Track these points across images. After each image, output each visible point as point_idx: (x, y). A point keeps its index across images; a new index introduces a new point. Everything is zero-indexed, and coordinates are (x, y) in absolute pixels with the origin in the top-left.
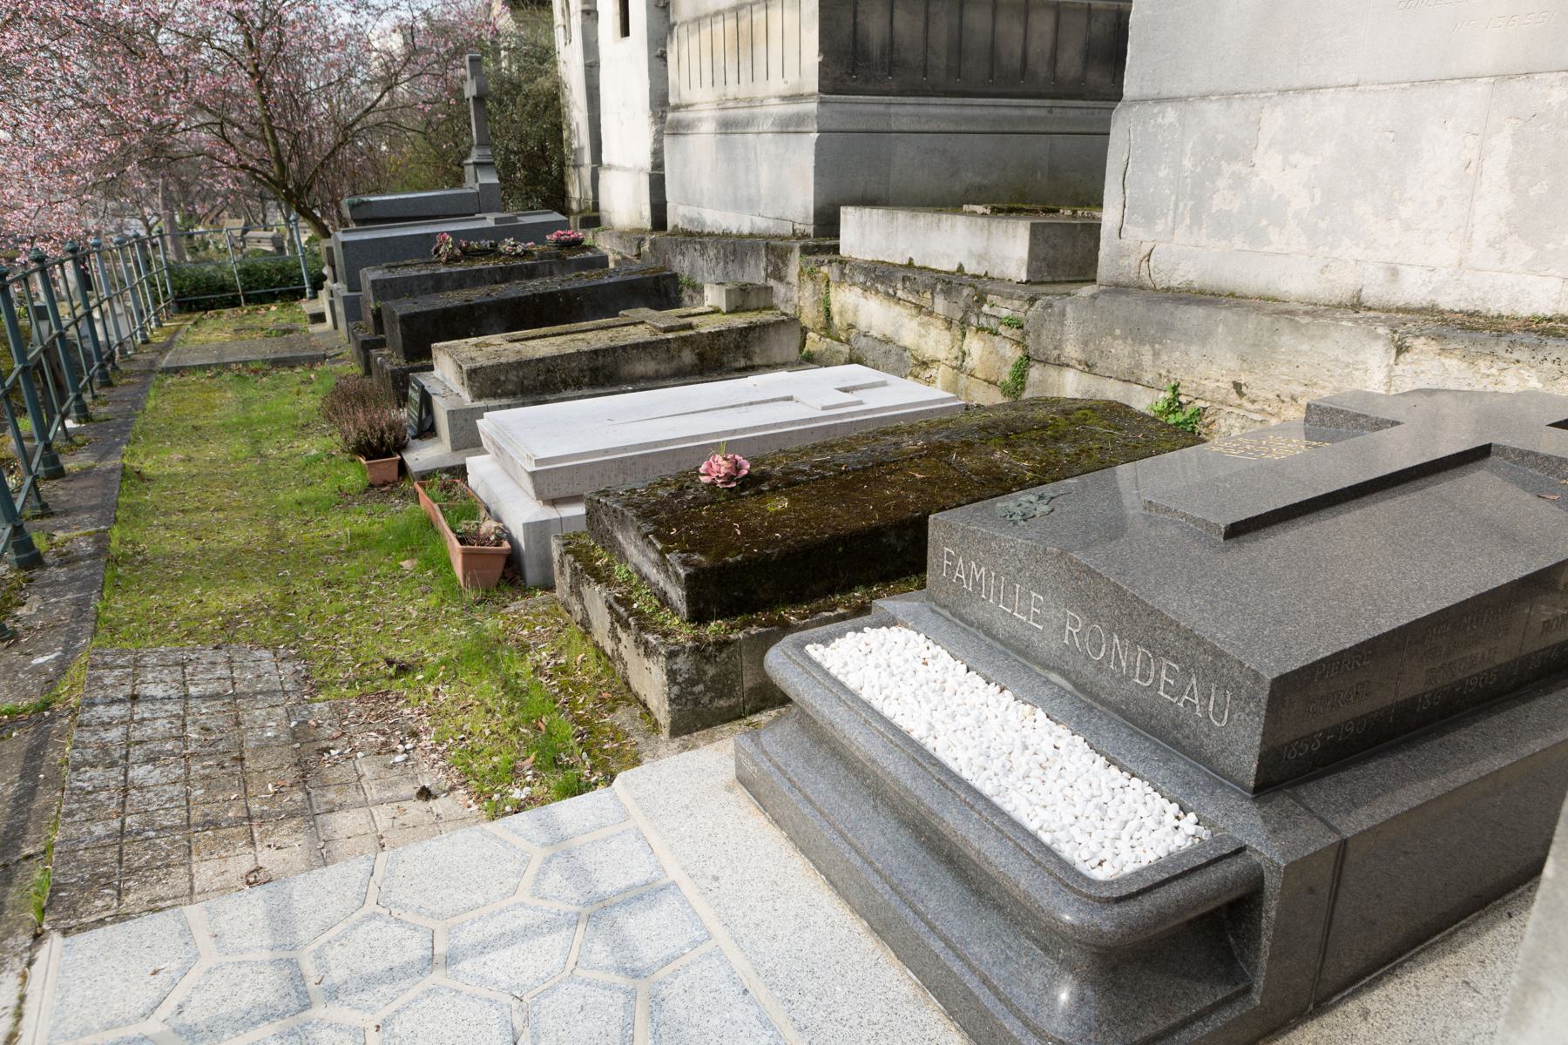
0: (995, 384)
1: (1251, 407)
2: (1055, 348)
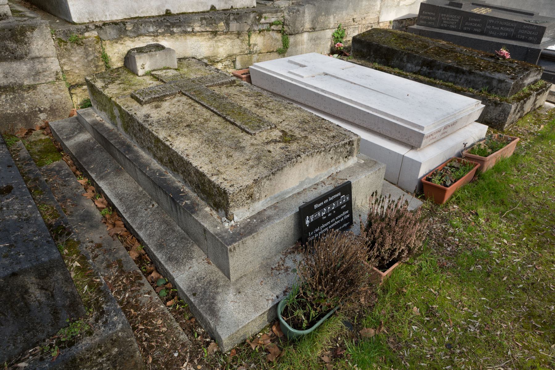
0: (273, 51)
1: (356, 24)
2: (302, 27)
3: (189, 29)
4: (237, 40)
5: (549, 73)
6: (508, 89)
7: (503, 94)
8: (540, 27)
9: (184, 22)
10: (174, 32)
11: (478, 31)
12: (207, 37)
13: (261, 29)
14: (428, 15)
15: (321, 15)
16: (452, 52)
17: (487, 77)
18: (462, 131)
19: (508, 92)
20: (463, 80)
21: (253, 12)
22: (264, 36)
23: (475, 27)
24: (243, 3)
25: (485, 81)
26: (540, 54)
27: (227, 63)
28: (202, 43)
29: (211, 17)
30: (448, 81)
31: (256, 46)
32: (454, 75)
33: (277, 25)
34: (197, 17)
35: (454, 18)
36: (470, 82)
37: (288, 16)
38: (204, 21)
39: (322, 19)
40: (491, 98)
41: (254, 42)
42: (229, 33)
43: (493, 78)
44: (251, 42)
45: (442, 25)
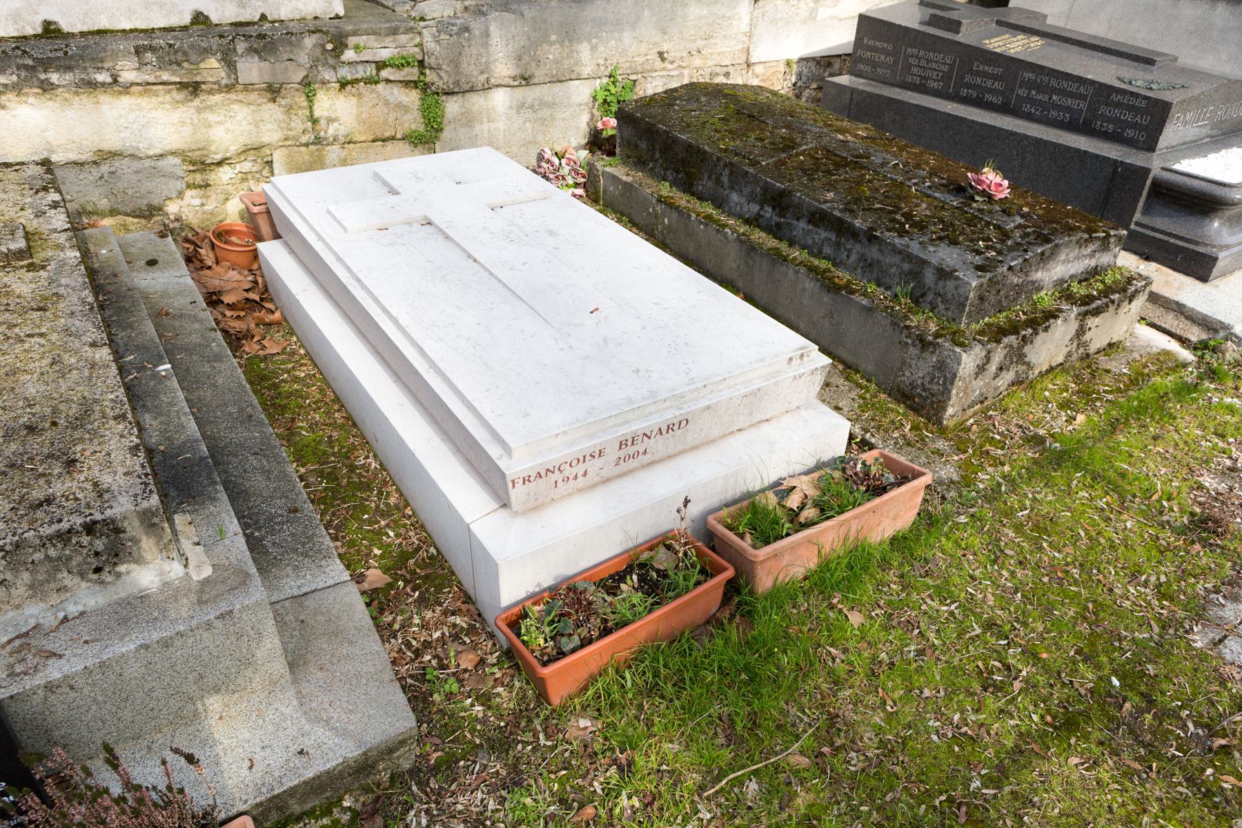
0: (393, 138)
1: (670, 66)
2: (482, 73)
3: (103, 77)
4: (271, 105)
5: (1172, 241)
6: (962, 299)
7: (950, 313)
8: (1157, 101)
9: (82, 57)
10: (52, 84)
11: (995, 100)
12: (168, 97)
13: (349, 78)
14: (874, 49)
15: (545, 39)
16: (857, 166)
17: (909, 257)
18: (736, 442)
19: (963, 311)
20: (853, 257)
21: (314, 32)
22: (360, 95)
23: (990, 91)
24: (300, 6)
25: (906, 267)
26: (1149, 182)
27: (247, 166)
28: (153, 114)
29: (170, 46)
30: (819, 255)
31: (336, 125)
32: (833, 238)
33: (400, 67)
34: (128, 45)
35: (935, 62)
36: (870, 265)
37: (433, 45)
38: (149, 55)
39: (552, 53)
40: (914, 321)
41: (326, 114)
42: (240, 87)
43: (924, 262)
44: (317, 114)
45: (909, 79)
